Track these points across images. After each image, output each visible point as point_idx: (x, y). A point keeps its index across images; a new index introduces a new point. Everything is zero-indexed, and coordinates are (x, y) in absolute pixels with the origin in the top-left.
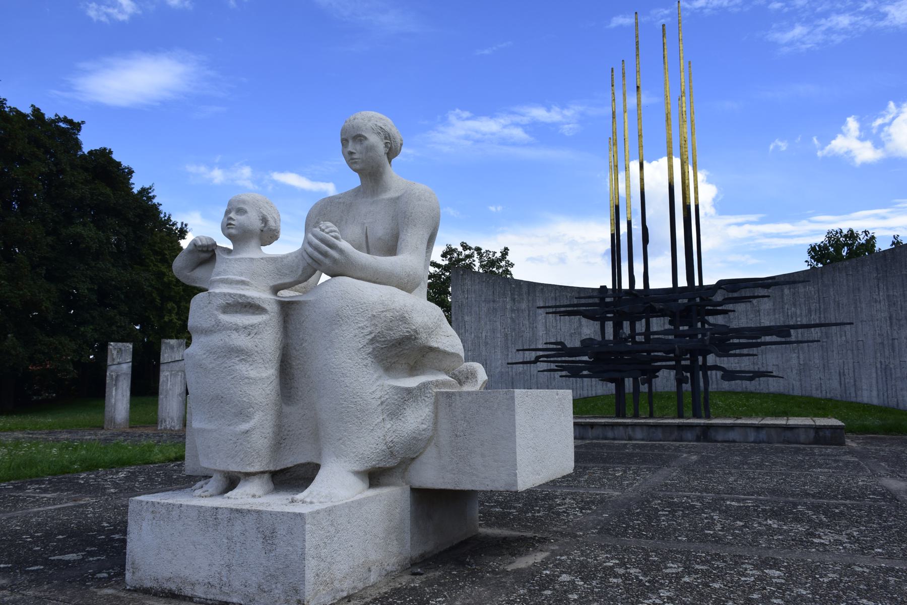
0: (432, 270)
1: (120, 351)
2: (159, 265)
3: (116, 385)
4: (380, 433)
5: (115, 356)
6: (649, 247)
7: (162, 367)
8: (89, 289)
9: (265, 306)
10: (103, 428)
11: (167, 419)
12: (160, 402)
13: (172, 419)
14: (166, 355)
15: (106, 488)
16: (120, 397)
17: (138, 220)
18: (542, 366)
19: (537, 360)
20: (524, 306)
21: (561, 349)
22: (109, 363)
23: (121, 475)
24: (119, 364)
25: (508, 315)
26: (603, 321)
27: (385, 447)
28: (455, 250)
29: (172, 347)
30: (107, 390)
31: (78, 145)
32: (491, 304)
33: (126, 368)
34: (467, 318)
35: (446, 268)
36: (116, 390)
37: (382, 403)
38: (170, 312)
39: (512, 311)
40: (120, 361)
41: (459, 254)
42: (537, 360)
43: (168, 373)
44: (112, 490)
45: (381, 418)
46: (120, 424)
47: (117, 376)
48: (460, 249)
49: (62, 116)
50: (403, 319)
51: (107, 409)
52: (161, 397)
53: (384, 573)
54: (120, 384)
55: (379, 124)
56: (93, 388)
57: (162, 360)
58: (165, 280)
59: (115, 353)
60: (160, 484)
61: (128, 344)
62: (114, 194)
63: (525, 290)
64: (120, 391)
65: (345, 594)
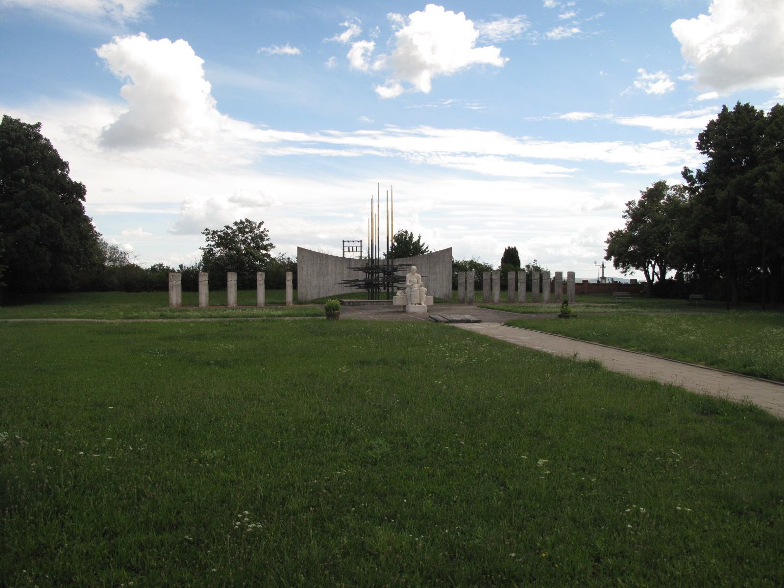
6: (379, 252)
16: (173, 294)
18: (345, 285)
19: (344, 283)
20: (324, 262)
21: (357, 281)
22: (170, 281)
25: (319, 265)
26: (366, 273)
32: (313, 262)
34: (303, 266)
39: (320, 264)
42: (344, 283)
63: (324, 257)
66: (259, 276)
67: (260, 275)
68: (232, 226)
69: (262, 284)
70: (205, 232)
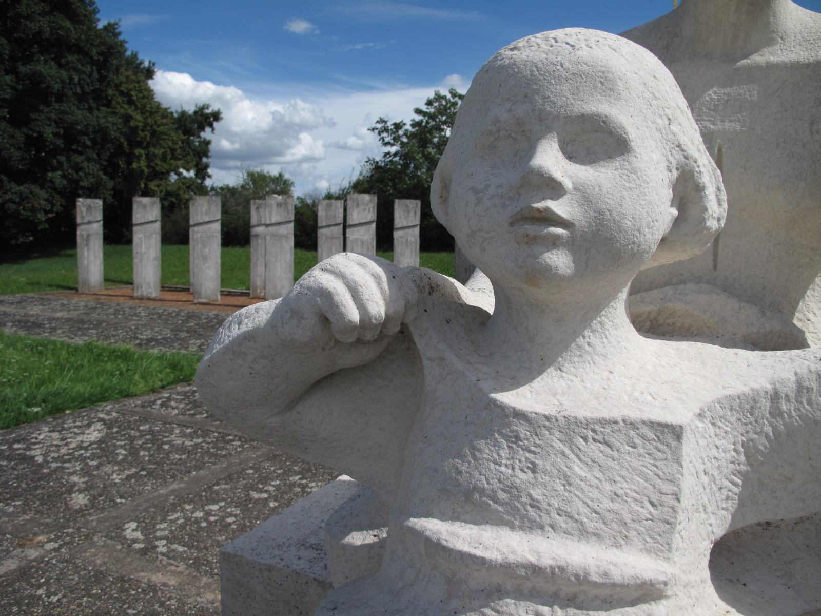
0: (418, 118)
1: (89, 208)
2: (126, 106)
3: (87, 245)
5: (84, 213)
7: (135, 229)
8: (55, 134)
10: (77, 290)
11: (144, 286)
12: (135, 267)
13: (149, 286)
15: (71, 489)
16: (92, 257)
17: (101, 58)
23: (94, 434)
24: (89, 223)
28: (444, 97)
29: (144, 207)
33: (97, 228)
35: (432, 117)
36: (88, 250)
38: (139, 157)
40: (90, 215)
41: (447, 101)
43: (141, 235)
44: (80, 500)
47: (88, 236)
48: (449, 96)
51: (80, 270)
52: (135, 261)
54: (92, 244)
58: (132, 124)
59: (84, 210)
60: (150, 474)
62: (75, 29)
64: (92, 252)
66: (274, 208)
67: (279, 205)
68: (424, 108)
69: (286, 237)
70: (379, 126)
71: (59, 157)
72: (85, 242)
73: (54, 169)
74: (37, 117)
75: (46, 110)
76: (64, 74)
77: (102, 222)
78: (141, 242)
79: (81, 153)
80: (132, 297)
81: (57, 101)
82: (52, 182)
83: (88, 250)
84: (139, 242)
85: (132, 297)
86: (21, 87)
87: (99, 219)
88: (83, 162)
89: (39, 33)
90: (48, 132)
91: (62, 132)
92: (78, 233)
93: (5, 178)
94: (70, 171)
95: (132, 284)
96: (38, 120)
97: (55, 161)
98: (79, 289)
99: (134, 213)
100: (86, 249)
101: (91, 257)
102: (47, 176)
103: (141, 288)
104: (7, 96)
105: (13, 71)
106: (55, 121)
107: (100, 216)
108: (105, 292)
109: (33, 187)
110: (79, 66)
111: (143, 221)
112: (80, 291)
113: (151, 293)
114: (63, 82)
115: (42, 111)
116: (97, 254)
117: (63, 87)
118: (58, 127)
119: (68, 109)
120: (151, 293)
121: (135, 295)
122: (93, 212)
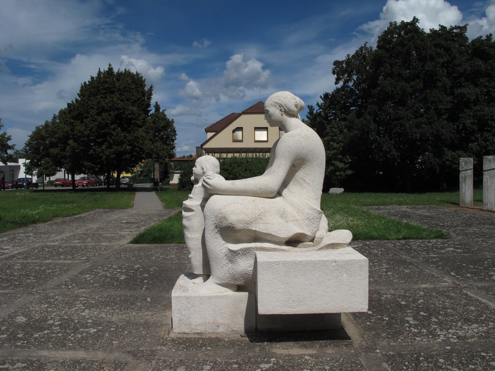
1: (466, 163)
3: (465, 182)
4: (226, 268)
5: (463, 165)
7: (484, 173)
9: (194, 209)
10: (459, 205)
11: (489, 204)
12: (484, 193)
14: (486, 166)
24: (466, 170)
27: (229, 275)
29: (490, 161)
30: (460, 184)
31: (467, 39)
36: (465, 185)
37: (226, 255)
43: (487, 176)
45: (226, 262)
46: (468, 204)
47: (465, 177)
49: (454, 26)
50: (225, 218)
52: (484, 190)
53: (230, 330)
54: (467, 181)
55: (275, 101)
56: (453, 185)
57: (484, 169)
59: (463, 163)
61: (470, 158)
64: (467, 185)
65: (199, 331)
71: (475, 135)
72: (464, 181)
73: (473, 142)
74: (463, 115)
75: (466, 110)
76: (478, 90)
77: (472, 170)
78: (488, 180)
79: (489, 131)
80: (482, 210)
81: (474, 106)
82: (472, 149)
83: (465, 185)
84: (486, 180)
85: (482, 210)
86: (456, 101)
87: (471, 168)
88: (489, 136)
89: (465, 70)
90: (468, 123)
91: (476, 121)
92: (460, 176)
93: (446, 149)
94: (482, 142)
95: (481, 201)
96: (463, 117)
97: (473, 137)
98: (460, 205)
99: (484, 164)
100: (464, 184)
101: (467, 189)
102: (469, 145)
103: (487, 205)
104: (448, 107)
105: (452, 94)
106: (473, 117)
107: (472, 167)
108: (473, 207)
109: (459, 152)
110: (487, 84)
111: (489, 169)
112: (460, 206)
113: (493, 208)
114: (477, 94)
115: (465, 112)
116: (470, 187)
117: (477, 98)
118: (474, 119)
119: (480, 109)
120: (493, 208)
121: (484, 209)
122: (468, 164)
